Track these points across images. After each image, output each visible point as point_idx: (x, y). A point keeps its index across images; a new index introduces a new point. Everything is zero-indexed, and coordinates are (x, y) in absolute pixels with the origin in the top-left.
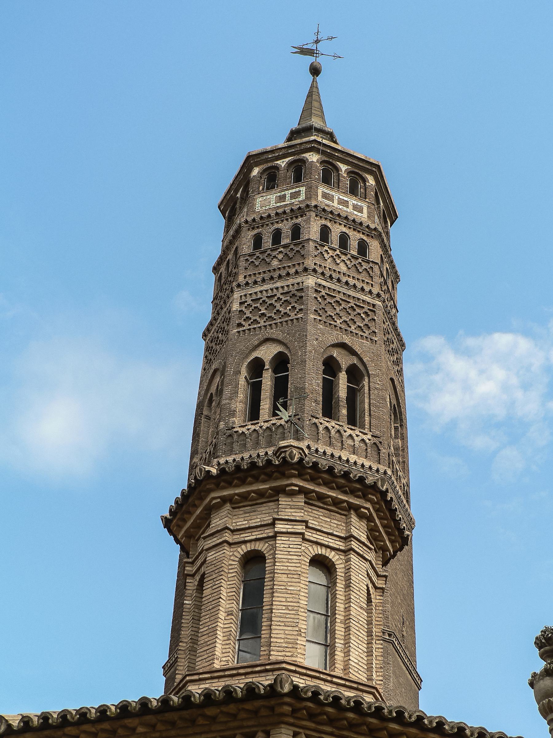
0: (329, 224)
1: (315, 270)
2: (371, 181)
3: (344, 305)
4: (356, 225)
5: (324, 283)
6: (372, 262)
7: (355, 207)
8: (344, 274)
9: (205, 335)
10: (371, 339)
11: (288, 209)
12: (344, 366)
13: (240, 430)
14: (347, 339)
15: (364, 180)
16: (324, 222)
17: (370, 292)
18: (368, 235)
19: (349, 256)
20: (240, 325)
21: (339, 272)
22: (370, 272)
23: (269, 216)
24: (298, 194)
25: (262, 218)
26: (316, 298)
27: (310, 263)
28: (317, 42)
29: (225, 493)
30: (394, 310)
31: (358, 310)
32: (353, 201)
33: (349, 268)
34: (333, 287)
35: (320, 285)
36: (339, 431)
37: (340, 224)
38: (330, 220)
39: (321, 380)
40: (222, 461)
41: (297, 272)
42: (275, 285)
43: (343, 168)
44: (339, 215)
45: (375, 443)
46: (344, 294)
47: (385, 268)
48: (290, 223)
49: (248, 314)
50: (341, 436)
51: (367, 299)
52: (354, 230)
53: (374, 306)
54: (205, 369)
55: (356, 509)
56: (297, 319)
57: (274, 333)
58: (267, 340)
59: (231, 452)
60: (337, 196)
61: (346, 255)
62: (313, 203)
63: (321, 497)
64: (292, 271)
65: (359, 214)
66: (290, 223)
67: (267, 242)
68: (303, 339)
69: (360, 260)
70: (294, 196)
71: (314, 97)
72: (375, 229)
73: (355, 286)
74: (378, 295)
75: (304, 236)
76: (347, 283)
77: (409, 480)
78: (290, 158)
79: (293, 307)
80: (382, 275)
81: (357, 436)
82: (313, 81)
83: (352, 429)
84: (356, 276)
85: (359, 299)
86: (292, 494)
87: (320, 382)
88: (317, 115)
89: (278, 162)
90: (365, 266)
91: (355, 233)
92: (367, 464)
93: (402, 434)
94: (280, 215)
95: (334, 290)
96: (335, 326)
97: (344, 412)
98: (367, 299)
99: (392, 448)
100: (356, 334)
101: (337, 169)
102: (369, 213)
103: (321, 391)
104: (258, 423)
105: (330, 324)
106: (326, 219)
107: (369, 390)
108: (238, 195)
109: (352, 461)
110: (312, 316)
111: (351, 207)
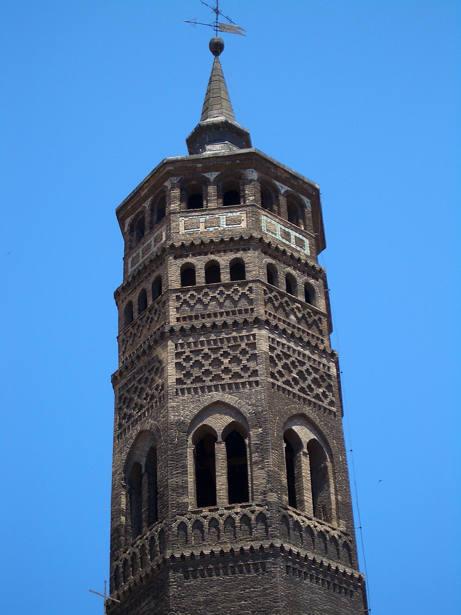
1: (267, 322)
8: (294, 327)
16: (270, 260)
48: (232, 256)
54: (120, 425)
66: (232, 256)
67: (200, 278)
75: (249, 277)
82: (216, 62)
83: (321, 524)
89: (207, 175)
101: (277, 191)
104: (218, 509)
108: (147, 204)
110: (272, 380)
111: (293, 240)
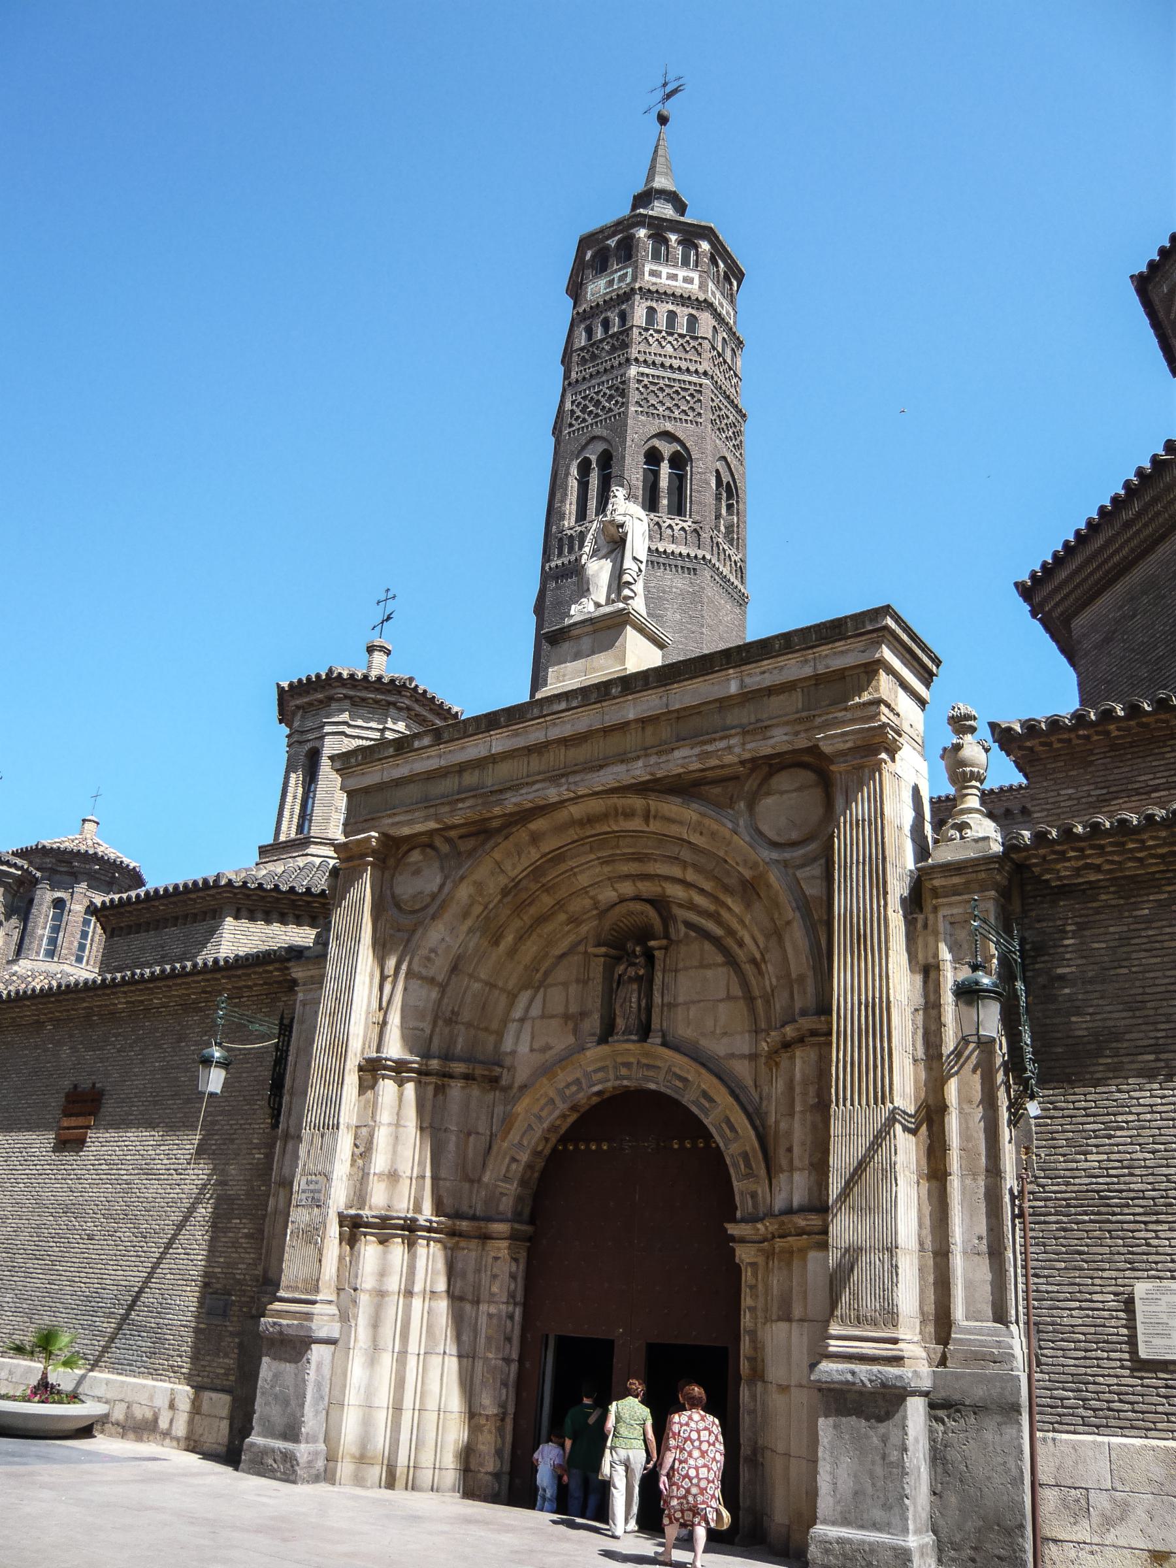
0: (654, 305)
1: (636, 360)
2: (705, 246)
3: (667, 390)
4: (684, 300)
5: (647, 371)
6: (701, 338)
7: (686, 280)
8: (670, 357)
9: (553, 433)
10: (697, 423)
11: (614, 295)
12: (666, 455)
13: (569, 532)
14: (669, 426)
15: (696, 247)
16: (649, 303)
17: (696, 372)
18: (698, 309)
19: (676, 336)
20: (571, 425)
21: (665, 356)
22: (699, 349)
23: (598, 304)
24: (626, 275)
25: (591, 307)
26: (638, 389)
27: (633, 353)
28: (665, 85)
29: (298, 702)
30: (735, 380)
31: (683, 393)
32: (682, 273)
33: (675, 350)
34: (656, 373)
35: (642, 374)
36: (658, 524)
37: (667, 303)
38: (657, 301)
39: (641, 473)
40: (553, 564)
41: (620, 364)
42: (602, 380)
43: (673, 238)
44: (665, 293)
45: (695, 530)
46: (669, 379)
47: (720, 339)
49: (579, 413)
50: (660, 527)
51: (694, 379)
52: (683, 305)
53: (701, 385)
55: (394, 704)
56: (619, 414)
57: (598, 431)
58: (594, 438)
59: (560, 554)
60: (665, 270)
61: (671, 334)
62: (637, 286)
63: (363, 699)
64: (616, 363)
65: (689, 286)
68: (623, 436)
69: (688, 338)
70: (622, 278)
71: (660, 152)
72: (705, 300)
73: (679, 368)
74: (705, 373)
76: (671, 367)
77: (744, 555)
78: (619, 236)
79: (617, 401)
80: (714, 348)
81: (677, 524)
84: (683, 355)
85: (684, 381)
86: (339, 700)
87: (640, 476)
88: (661, 174)
89: (608, 242)
90: (693, 343)
91: (683, 309)
92: (685, 552)
93: (738, 510)
94: (609, 304)
95: (658, 376)
96: (658, 415)
97: (665, 502)
98: (694, 379)
99: (722, 529)
100: (681, 419)
102: (701, 283)
103: (640, 484)
105: (653, 414)
106: (652, 300)
107: (691, 476)
109: (669, 551)
111: (680, 278)
